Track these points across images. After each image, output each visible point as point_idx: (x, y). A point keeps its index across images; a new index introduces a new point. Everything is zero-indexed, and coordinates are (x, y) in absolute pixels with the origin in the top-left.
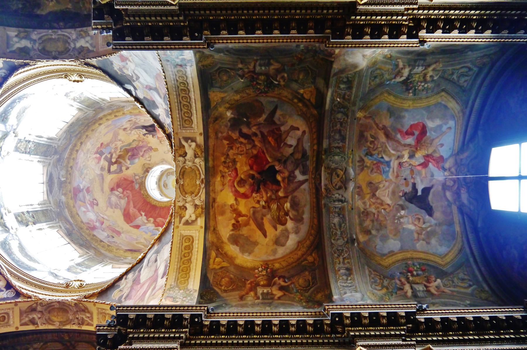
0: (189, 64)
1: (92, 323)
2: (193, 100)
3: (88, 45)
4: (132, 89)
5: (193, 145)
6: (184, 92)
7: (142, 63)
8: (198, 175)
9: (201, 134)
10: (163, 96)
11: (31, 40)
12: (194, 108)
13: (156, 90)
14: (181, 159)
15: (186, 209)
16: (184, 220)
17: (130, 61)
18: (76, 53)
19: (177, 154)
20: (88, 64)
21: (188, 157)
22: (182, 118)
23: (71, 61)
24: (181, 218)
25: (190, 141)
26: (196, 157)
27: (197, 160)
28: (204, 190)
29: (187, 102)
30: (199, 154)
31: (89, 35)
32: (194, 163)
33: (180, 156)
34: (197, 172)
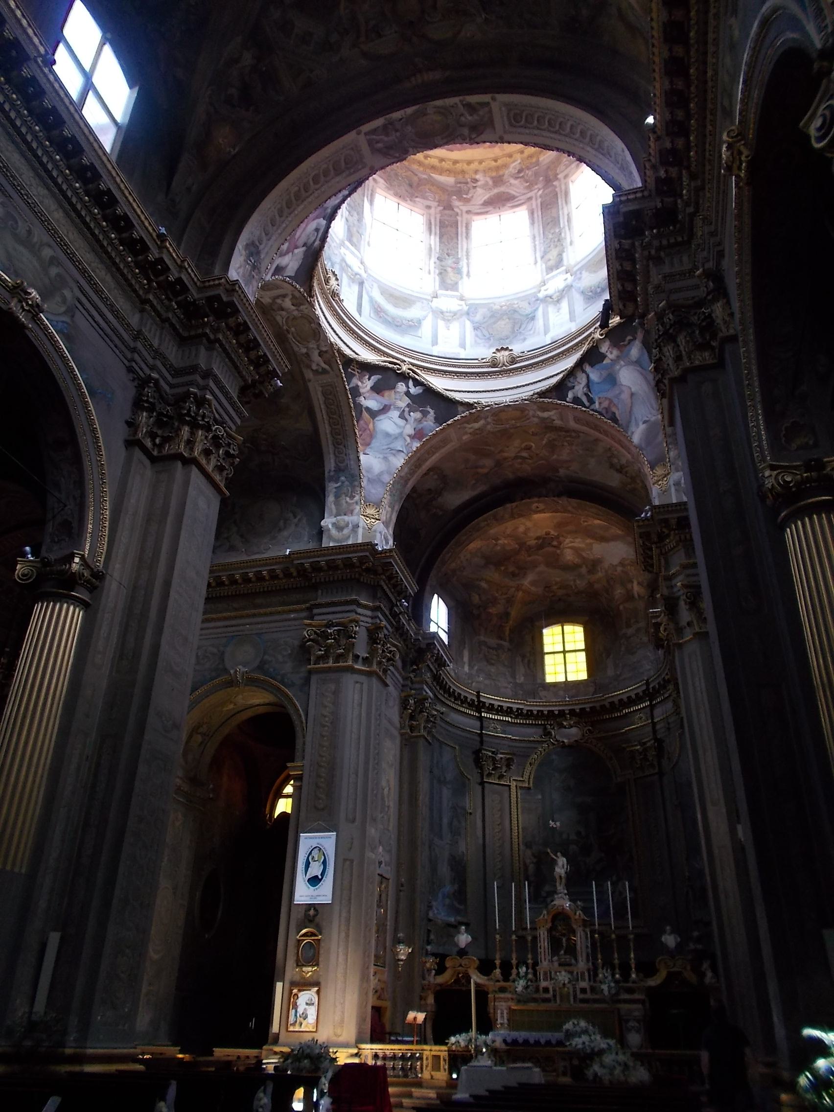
0: (332, 474)
1: (368, 137)
2: (326, 422)
3: (470, 426)
4: (413, 390)
5: (314, 367)
6: (337, 431)
7: (391, 446)
8: (295, 335)
9: (310, 381)
10: (364, 412)
11: (538, 417)
12: (324, 412)
13: (373, 414)
14: (324, 349)
15: (293, 305)
16: (290, 297)
17: (409, 436)
18: (482, 415)
19: (331, 353)
20: (469, 406)
21: (316, 353)
22: (335, 395)
23: (488, 406)
24: (294, 297)
25: (320, 370)
26: (307, 354)
27: (304, 351)
28: (281, 323)
29: (333, 418)
30: (304, 358)
31: (470, 433)
32: (307, 348)
33: (326, 352)
34: (298, 339)
